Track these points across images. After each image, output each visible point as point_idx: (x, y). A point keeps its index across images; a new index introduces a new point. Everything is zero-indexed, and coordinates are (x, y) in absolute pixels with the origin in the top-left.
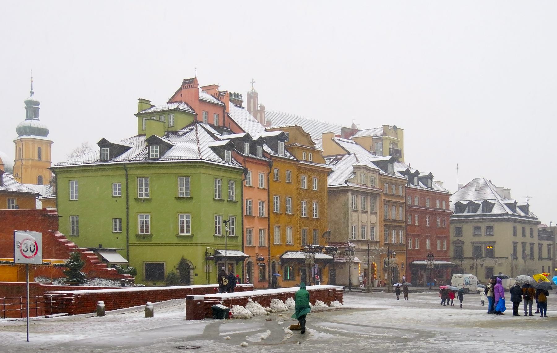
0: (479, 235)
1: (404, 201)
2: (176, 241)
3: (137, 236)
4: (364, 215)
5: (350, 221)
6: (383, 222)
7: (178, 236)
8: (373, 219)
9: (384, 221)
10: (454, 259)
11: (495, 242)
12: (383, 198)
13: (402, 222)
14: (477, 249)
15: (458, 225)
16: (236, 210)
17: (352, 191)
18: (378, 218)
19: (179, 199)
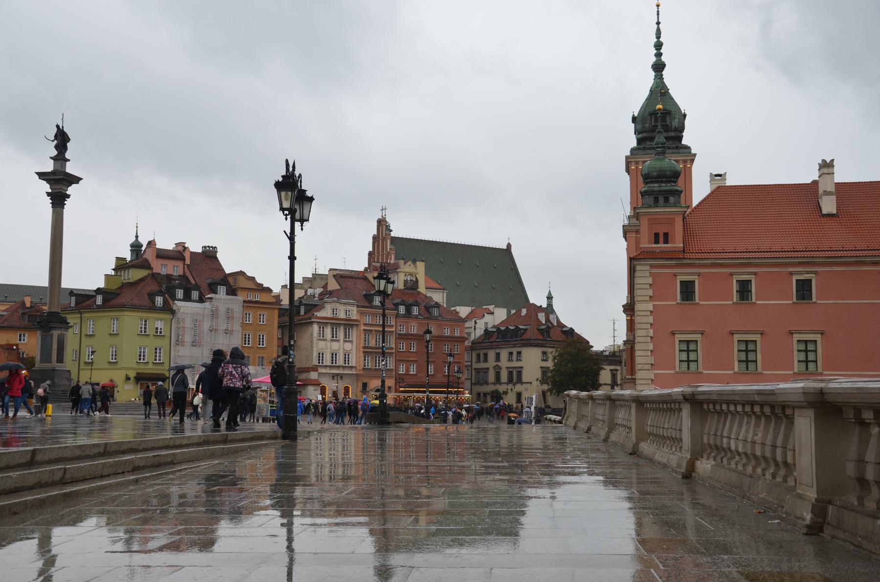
0: (512, 360)
1: (393, 329)
2: (107, 366)
3: (85, 363)
4: (336, 344)
5: (315, 349)
6: (362, 350)
7: (109, 363)
8: (348, 346)
9: (364, 348)
10: (494, 384)
11: (522, 367)
12: (363, 327)
13: (392, 349)
14: (510, 374)
15: (498, 351)
16: (163, 343)
17: (318, 322)
18: (355, 345)
19: (111, 335)
